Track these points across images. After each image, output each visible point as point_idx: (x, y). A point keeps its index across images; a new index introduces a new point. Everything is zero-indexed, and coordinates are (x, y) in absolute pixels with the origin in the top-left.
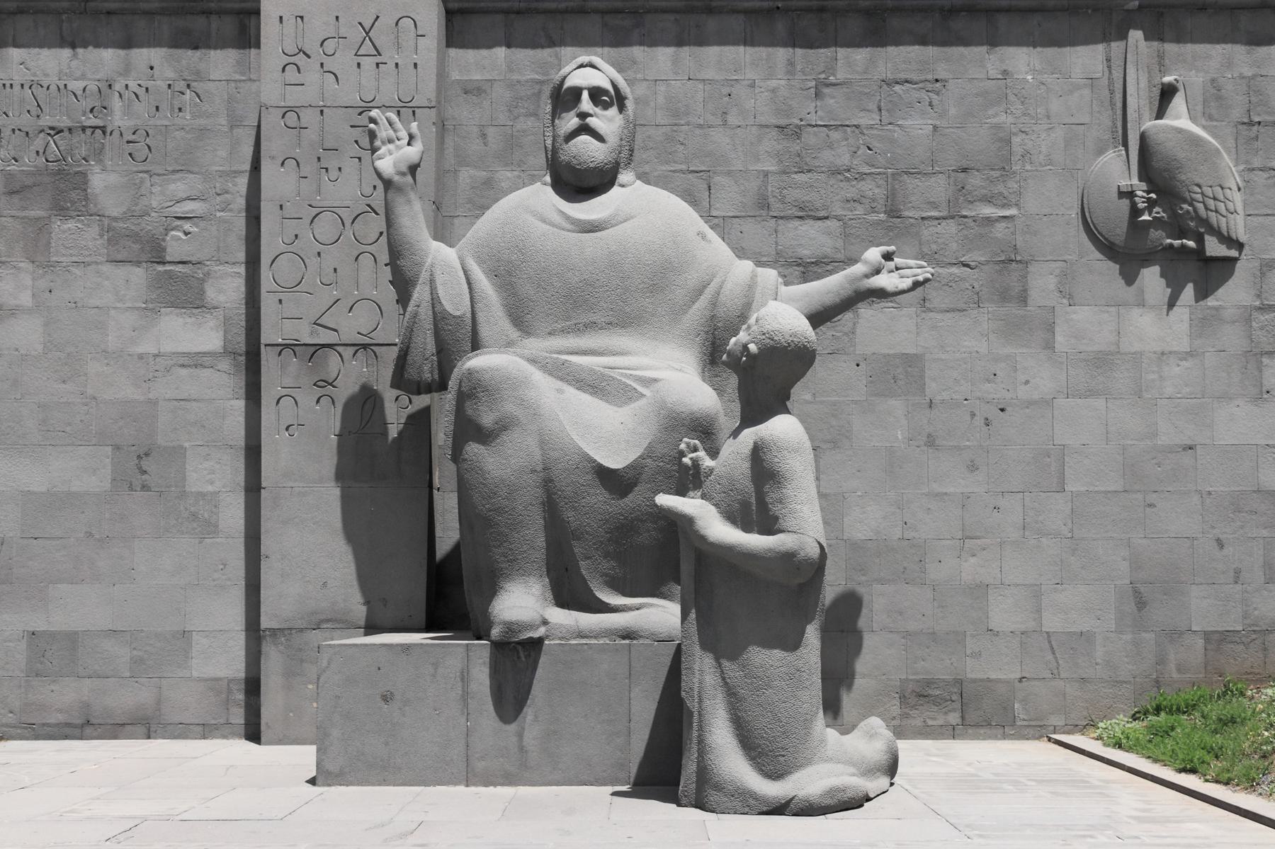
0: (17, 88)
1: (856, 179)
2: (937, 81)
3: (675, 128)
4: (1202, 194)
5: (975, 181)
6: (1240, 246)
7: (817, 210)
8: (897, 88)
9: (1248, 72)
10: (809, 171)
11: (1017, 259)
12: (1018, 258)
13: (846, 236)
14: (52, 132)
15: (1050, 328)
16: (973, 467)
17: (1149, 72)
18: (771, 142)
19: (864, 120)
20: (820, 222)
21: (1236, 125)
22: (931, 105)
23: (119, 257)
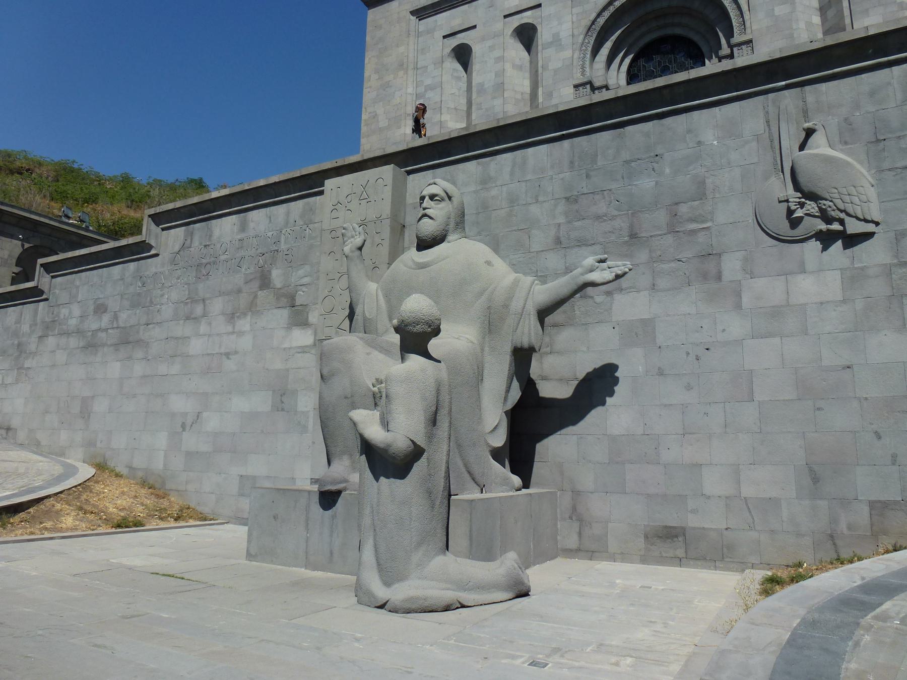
0: (251, 238)
2: (657, 155)
3: (511, 208)
5: (683, 209)
6: (877, 224)
7: (588, 240)
8: (633, 164)
9: (871, 109)
11: (713, 253)
12: (714, 252)
14: (261, 255)
15: (739, 295)
16: (689, 388)
17: (797, 123)
18: (562, 207)
19: (613, 186)
20: (590, 247)
21: (866, 145)
22: (653, 169)
23: (280, 305)
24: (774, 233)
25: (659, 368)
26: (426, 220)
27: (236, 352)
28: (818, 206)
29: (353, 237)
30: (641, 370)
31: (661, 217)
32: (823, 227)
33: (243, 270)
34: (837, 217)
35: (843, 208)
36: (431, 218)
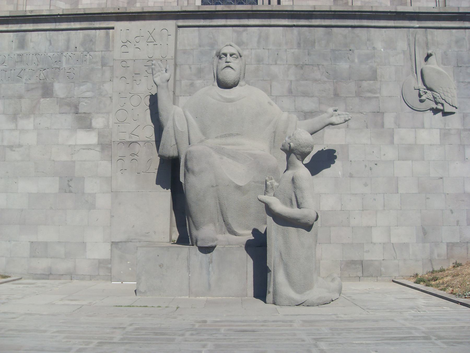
0: (31, 55)
1: (323, 83)
2: (350, 50)
3: (258, 65)
4: (443, 90)
5: (365, 84)
6: (456, 108)
8: (337, 52)
10: (306, 80)
13: (320, 103)
14: (42, 70)
15: (392, 136)
16: (366, 185)
22: (348, 58)
25: (350, 174)
26: (229, 70)
27: (20, 146)
28: (432, 95)
29: (159, 71)
30: (340, 174)
31: (352, 86)
32: (434, 106)
33: (24, 80)
34: (441, 102)
35: (444, 99)
36: (232, 68)
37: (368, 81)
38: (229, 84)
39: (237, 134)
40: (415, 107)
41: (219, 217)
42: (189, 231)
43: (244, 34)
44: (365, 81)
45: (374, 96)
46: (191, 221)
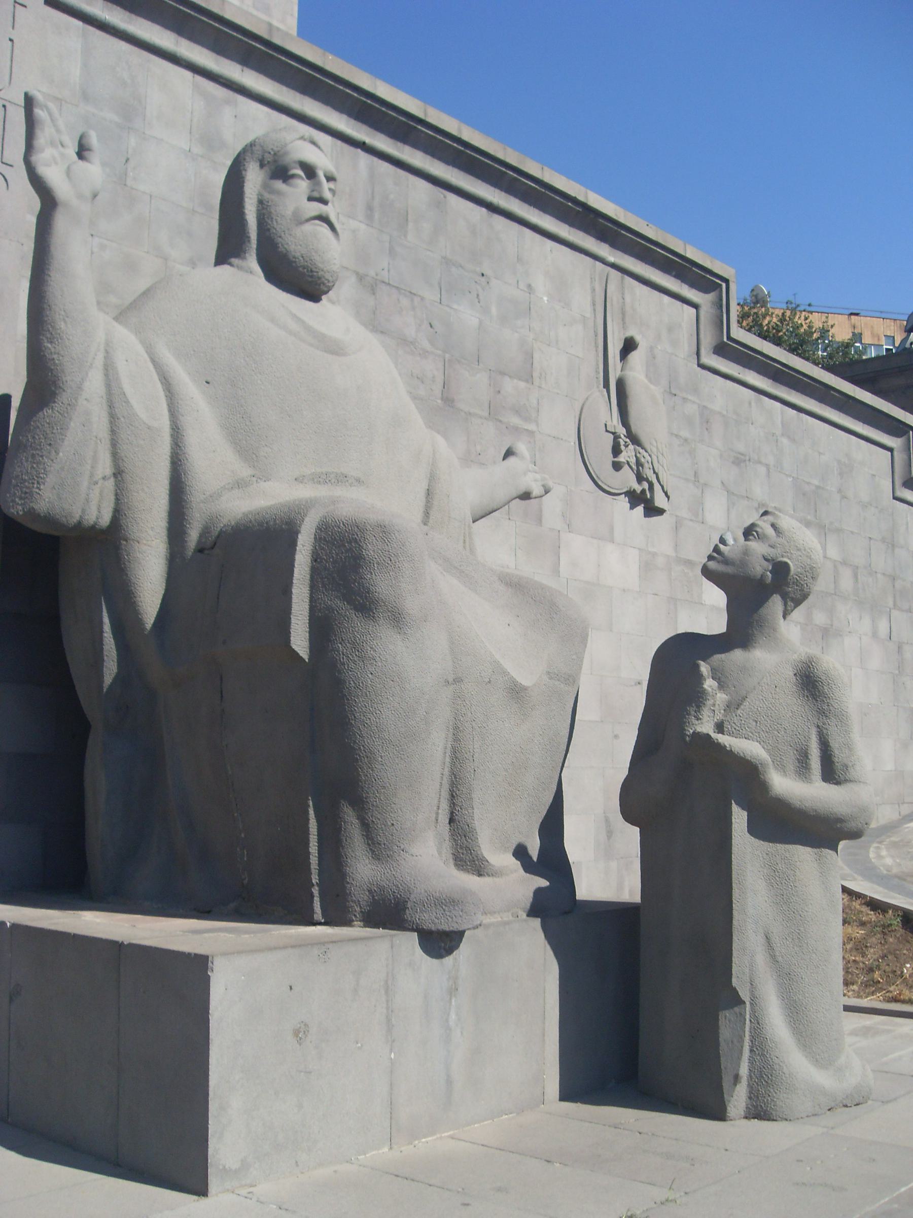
5: (510, 386)
8: (454, 269)
10: (382, 332)
22: (478, 295)
24: (596, 474)
26: (324, 229)
28: (636, 456)
29: (52, 144)
34: (650, 479)
37: (515, 381)
38: (324, 284)
39: (358, 480)
40: (602, 479)
41: (440, 806)
42: (319, 865)
43: (227, 114)
44: (510, 377)
45: (526, 428)
46: (356, 821)
